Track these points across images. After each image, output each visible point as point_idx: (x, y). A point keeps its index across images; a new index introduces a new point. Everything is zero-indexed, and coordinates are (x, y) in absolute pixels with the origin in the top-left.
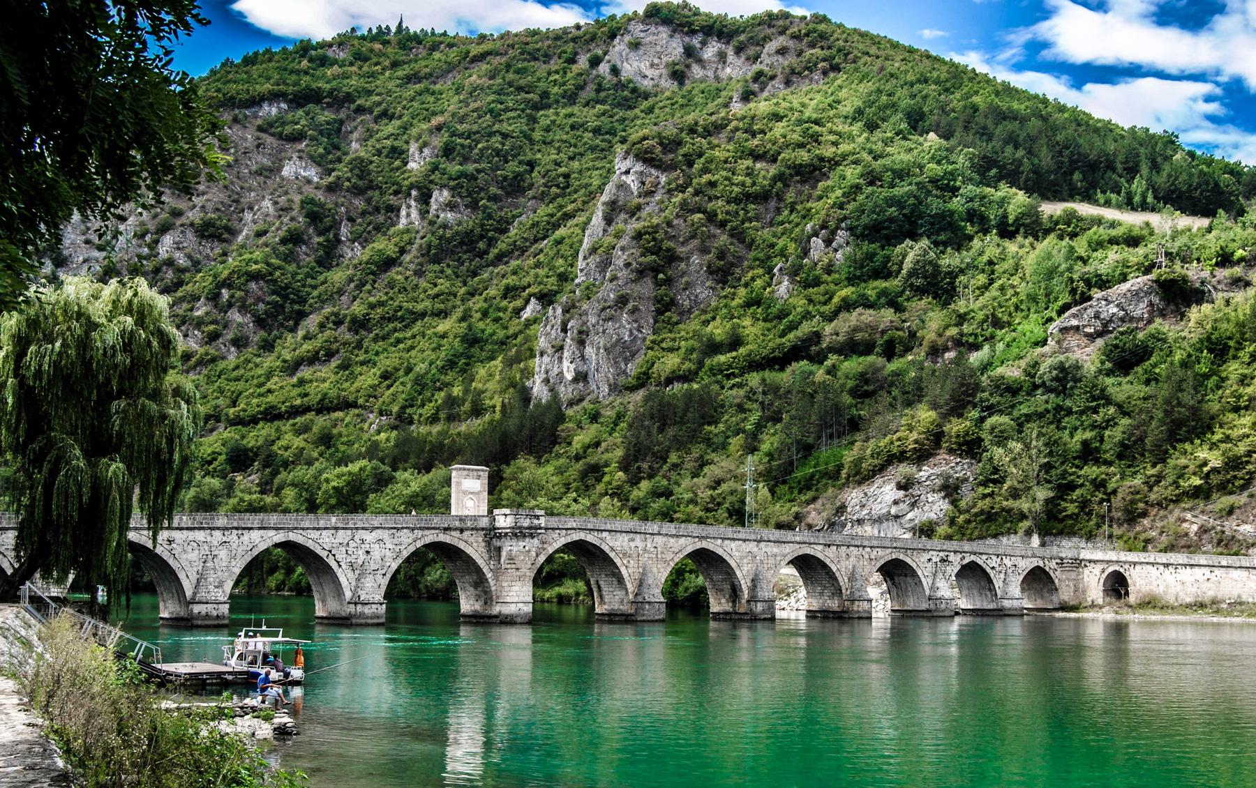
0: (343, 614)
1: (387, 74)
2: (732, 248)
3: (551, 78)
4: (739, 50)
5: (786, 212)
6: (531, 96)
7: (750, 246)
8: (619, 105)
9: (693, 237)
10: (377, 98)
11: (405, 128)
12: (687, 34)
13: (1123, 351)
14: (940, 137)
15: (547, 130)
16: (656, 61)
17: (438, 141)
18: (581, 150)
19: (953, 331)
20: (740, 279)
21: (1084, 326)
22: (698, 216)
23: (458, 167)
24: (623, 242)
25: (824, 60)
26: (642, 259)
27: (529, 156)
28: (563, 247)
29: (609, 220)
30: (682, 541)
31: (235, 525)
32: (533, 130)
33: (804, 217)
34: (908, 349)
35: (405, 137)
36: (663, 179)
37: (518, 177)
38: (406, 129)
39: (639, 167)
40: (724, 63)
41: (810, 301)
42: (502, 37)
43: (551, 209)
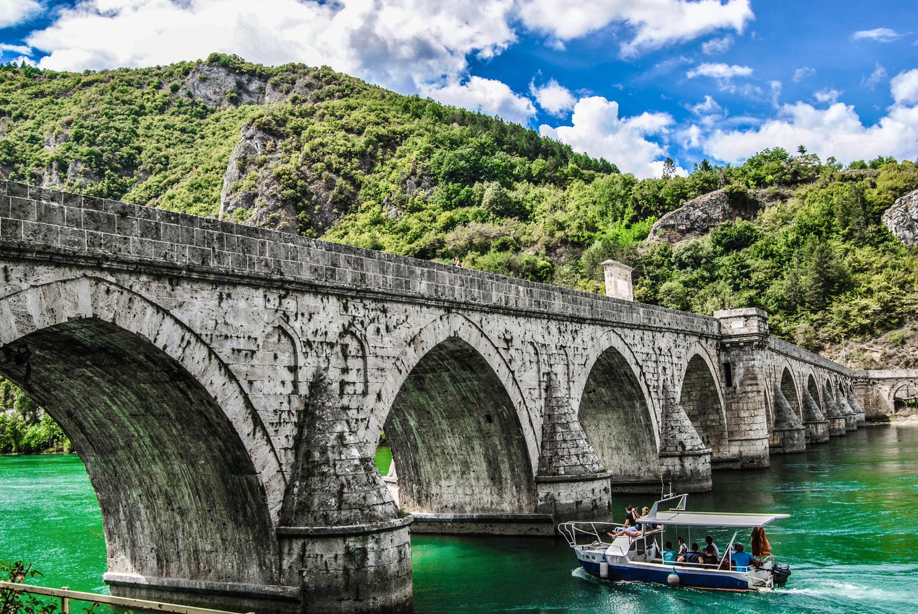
0: (645, 476)
1: (19, 91)
2: (348, 186)
3: (146, 96)
4: (275, 86)
5: (379, 164)
6: (133, 107)
7: (358, 186)
8: (196, 116)
9: (320, 177)
10: (16, 106)
11: (39, 124)
12: (238, 74)
13: (731, 238)
14: (460, 125)
15: (148, 128)
16: (218, 90)
17: (70, 132)
18: (174, 141)
19: (559, 234)
20: (356, 208)
21: (678, 225)
22: (319, 165)
23: (87, 148)
24: (267, 181)
25: (339, 91)
26: (285, 192)
27: (137, 144)
28: (175, 201)
29: (242, 170)
30: (781, 358)
31: (570, 312)
32: (137, 128)
33: (393, 168)
34: (517, 250)
35: (40, 130)
36: (280, 143)
37: (131, 157)
38: (39, 124)
39: (260, 134)
40: (264, 93)
41: (421, 220)
42: (102, 73)
43: (159, 177)
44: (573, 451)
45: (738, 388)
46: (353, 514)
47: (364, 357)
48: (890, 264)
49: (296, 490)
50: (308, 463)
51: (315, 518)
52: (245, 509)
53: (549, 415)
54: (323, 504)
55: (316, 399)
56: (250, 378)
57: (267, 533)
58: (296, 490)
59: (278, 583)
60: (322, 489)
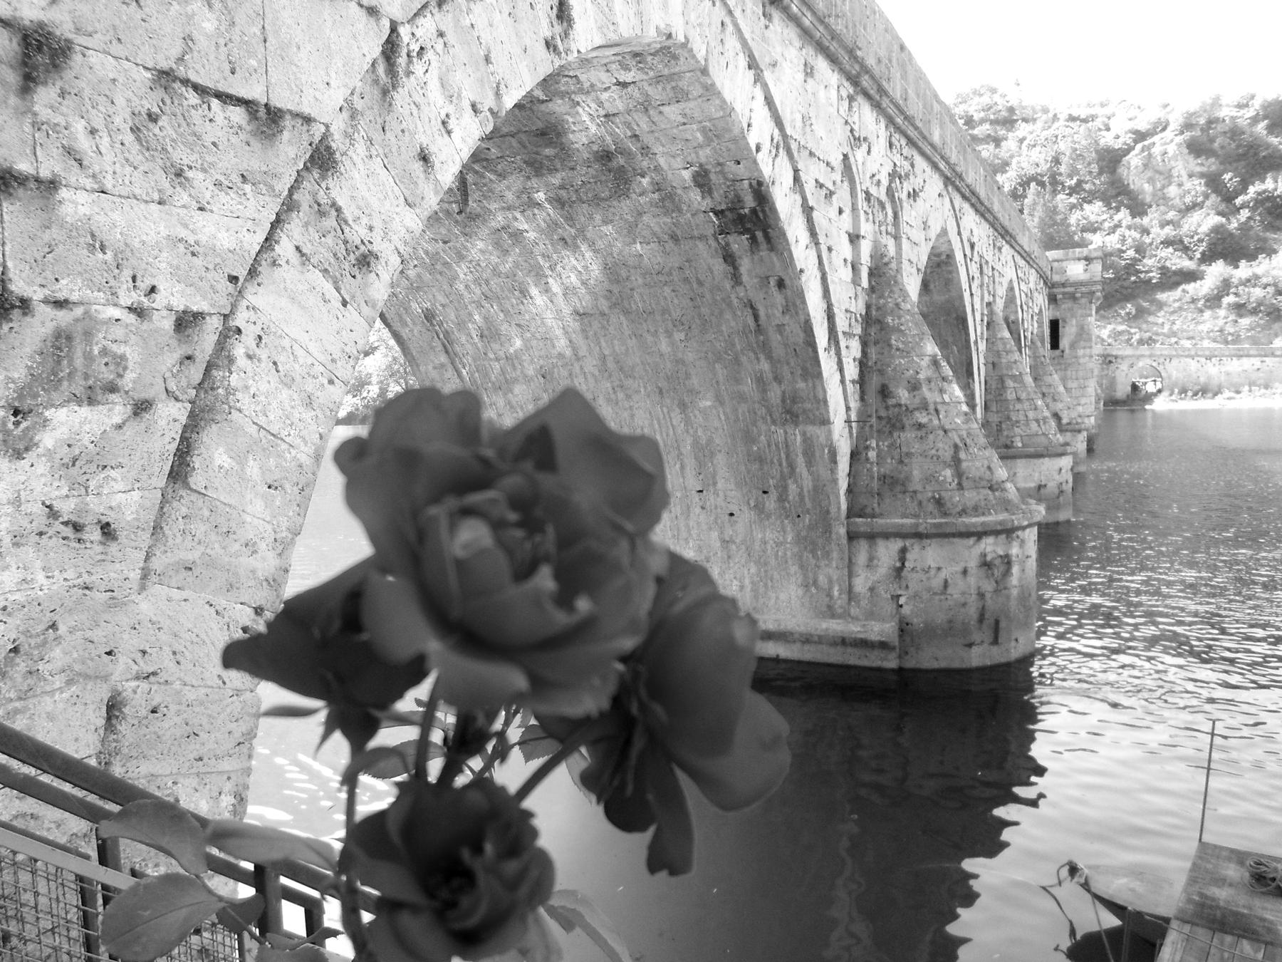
44: (1031, 414)
45: (1067, 351)
46: (982, 497)
47: (897, 238)
48: (1124, 224)
49: (872, 455)
50: (887, 408)
51: (920, 503)
52: (785, 488)
53: (994, 364)
54: (929, 479)
55: (882, 297)
56: (830, 243)
57: (828, 530)
58: (872, 455)
59: (845, 615)
60: (924, 455)
